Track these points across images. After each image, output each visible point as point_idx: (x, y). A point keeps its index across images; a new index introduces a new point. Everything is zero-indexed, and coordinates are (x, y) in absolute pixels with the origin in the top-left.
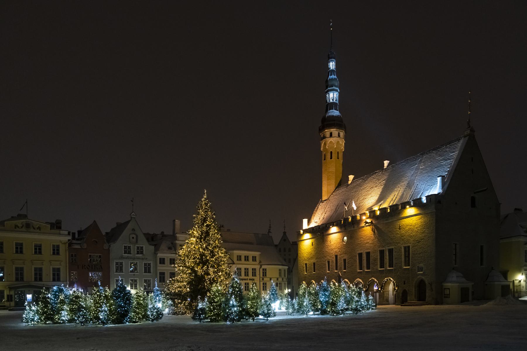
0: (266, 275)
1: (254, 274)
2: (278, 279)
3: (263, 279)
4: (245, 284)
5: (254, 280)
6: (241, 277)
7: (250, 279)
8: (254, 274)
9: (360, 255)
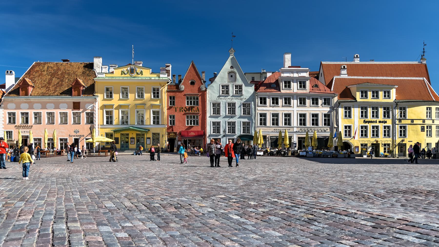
1: (386, 114)
4: (373, 127)
5: (386, 122)
6: (366, 120)
7: (380, 122)
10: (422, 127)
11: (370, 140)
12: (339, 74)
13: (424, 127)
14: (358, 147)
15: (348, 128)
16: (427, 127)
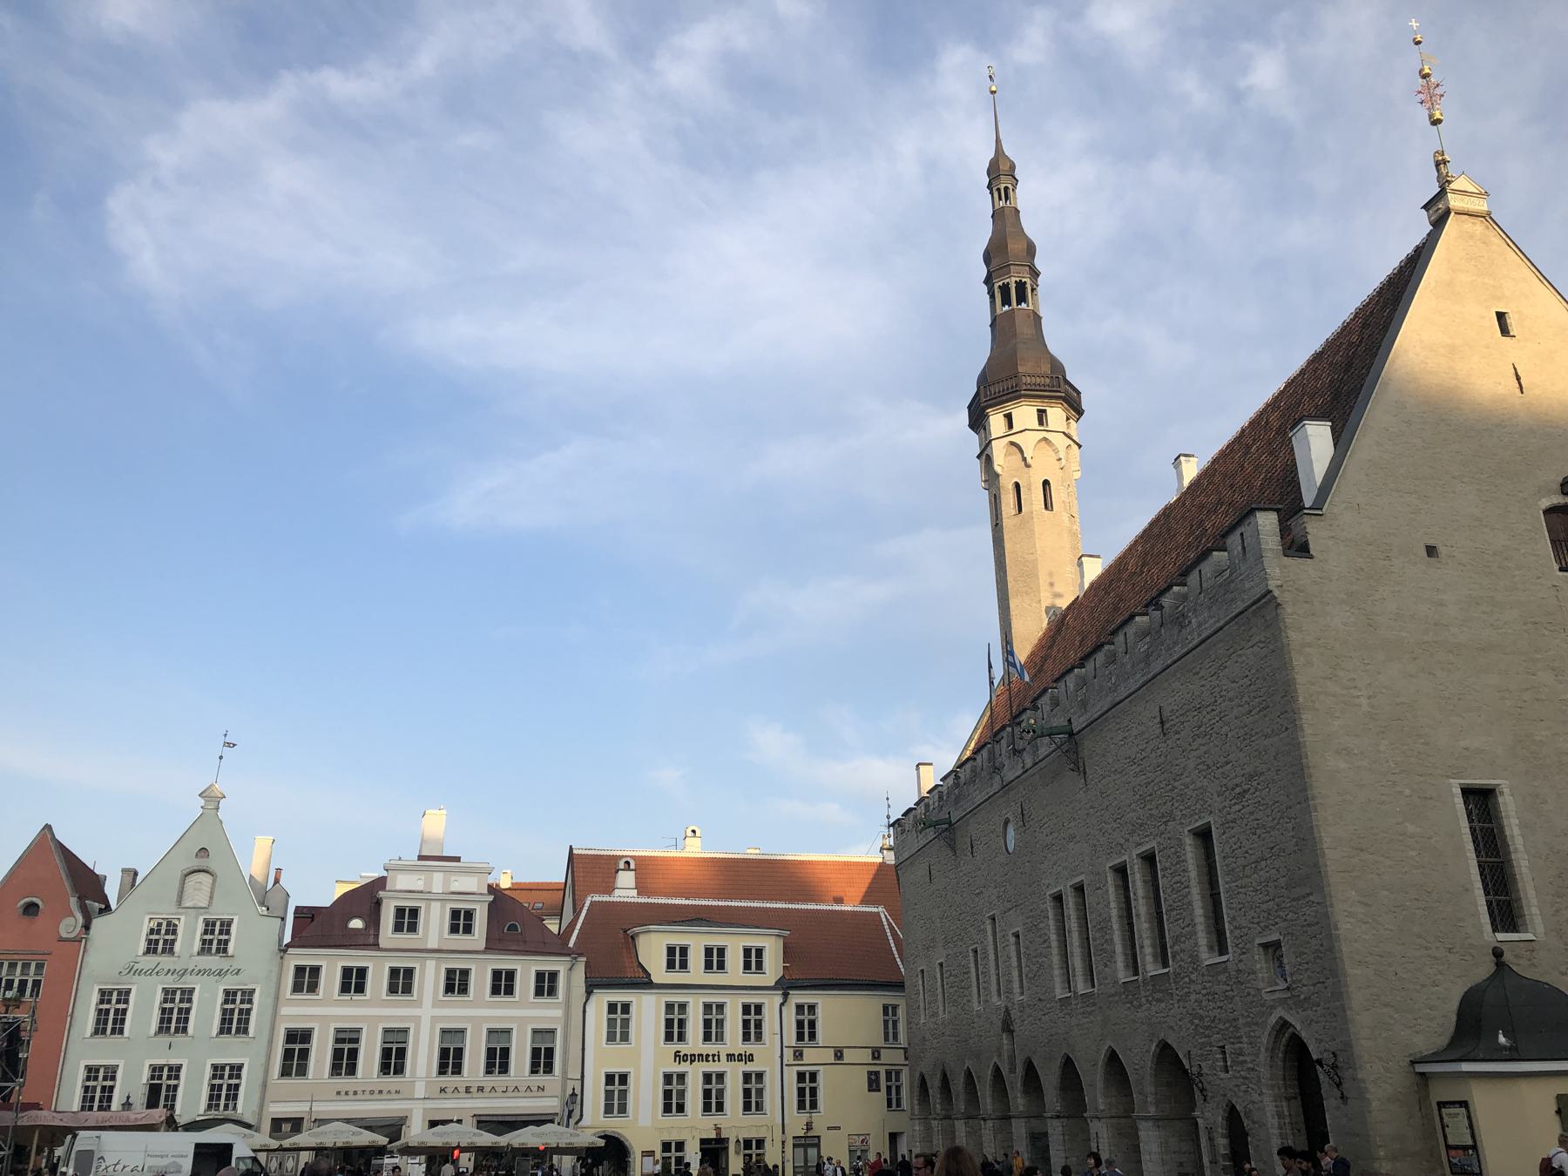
0: (812, 1036)
1: (752, 1028)
2: (876, 1053)
3: (798, 1055)
4: (707, 1078)
5: (750, 1058)
6: (685, 1049)
7: (730, 1057)
8: (752, 1028)
9: (1058, 898)
10: (870, 1073)
11: (694, 1126)
12: (610, 889)
13: (877, 1073)
14: (651, 1153)
15: (617, 1081)
16: (888, 1073)
